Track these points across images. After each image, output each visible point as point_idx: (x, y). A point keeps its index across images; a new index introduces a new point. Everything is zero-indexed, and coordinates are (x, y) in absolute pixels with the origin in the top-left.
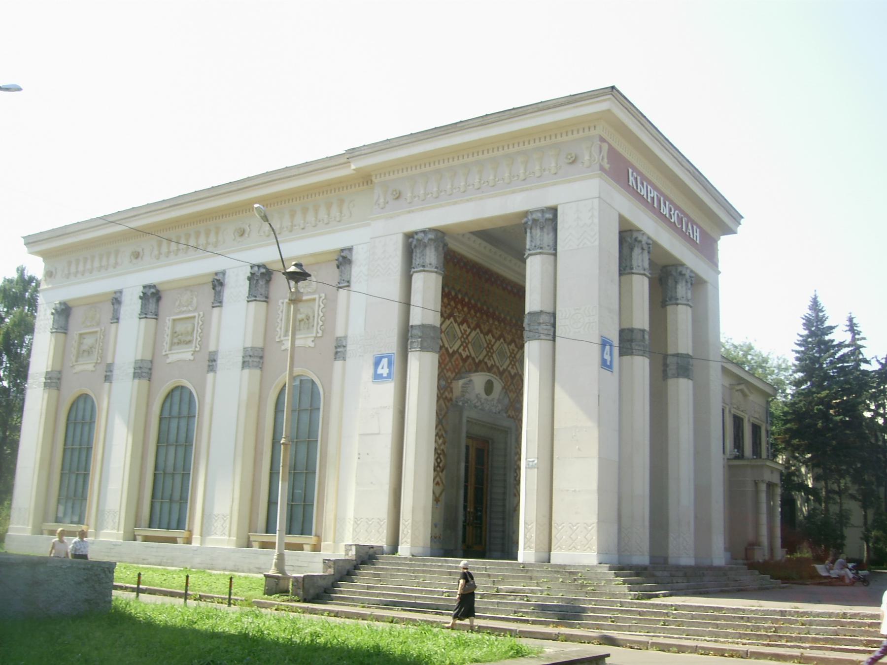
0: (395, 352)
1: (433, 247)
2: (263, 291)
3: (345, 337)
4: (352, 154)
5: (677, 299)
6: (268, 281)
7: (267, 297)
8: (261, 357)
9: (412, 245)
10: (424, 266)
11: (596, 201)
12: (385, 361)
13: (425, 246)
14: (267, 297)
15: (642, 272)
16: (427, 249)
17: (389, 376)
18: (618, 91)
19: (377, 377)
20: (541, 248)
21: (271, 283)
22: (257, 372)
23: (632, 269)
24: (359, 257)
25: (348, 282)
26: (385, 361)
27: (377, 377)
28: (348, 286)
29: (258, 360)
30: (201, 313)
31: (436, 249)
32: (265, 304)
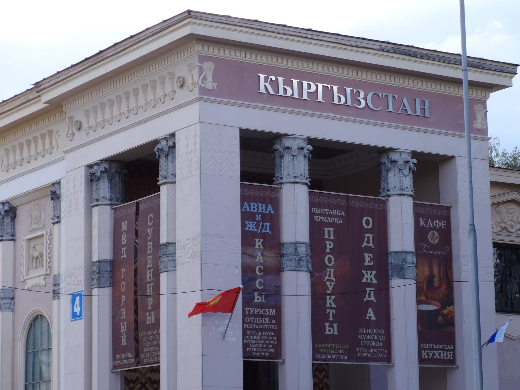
0: (83, 289)
1: (106, 179)
2: (9, 229)
3: (59, 275)
4: (39, 87)
5: (388, 190)
6: (14, 218)
7: (13, 236)
8: (13, 298)
9: (92, 179)
10: (97, 200)
11: (198, 125)
12: (78, 298)
13: (99, 179)
14: (13, 236)
15: (292, 180)
16: (101, 182)
17: (81, 315)
18: (194, 12)
19: (74, 316)
20: (165, 178)
21: (17, 219)
22: (9, 314)
23: (282, 178)
24: (63, 191)
25: (58, 217)
26: (78, 298)
27: (74, 316)
28: (59, 222)
29: (9, 301)
30: (48, 230)
31: (111, 180)
32: (11, 242)
